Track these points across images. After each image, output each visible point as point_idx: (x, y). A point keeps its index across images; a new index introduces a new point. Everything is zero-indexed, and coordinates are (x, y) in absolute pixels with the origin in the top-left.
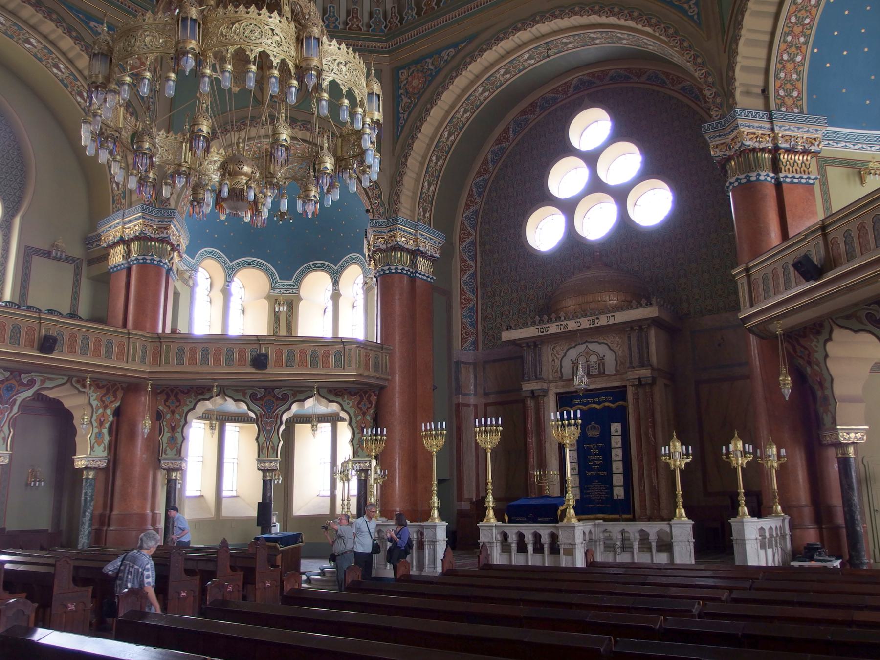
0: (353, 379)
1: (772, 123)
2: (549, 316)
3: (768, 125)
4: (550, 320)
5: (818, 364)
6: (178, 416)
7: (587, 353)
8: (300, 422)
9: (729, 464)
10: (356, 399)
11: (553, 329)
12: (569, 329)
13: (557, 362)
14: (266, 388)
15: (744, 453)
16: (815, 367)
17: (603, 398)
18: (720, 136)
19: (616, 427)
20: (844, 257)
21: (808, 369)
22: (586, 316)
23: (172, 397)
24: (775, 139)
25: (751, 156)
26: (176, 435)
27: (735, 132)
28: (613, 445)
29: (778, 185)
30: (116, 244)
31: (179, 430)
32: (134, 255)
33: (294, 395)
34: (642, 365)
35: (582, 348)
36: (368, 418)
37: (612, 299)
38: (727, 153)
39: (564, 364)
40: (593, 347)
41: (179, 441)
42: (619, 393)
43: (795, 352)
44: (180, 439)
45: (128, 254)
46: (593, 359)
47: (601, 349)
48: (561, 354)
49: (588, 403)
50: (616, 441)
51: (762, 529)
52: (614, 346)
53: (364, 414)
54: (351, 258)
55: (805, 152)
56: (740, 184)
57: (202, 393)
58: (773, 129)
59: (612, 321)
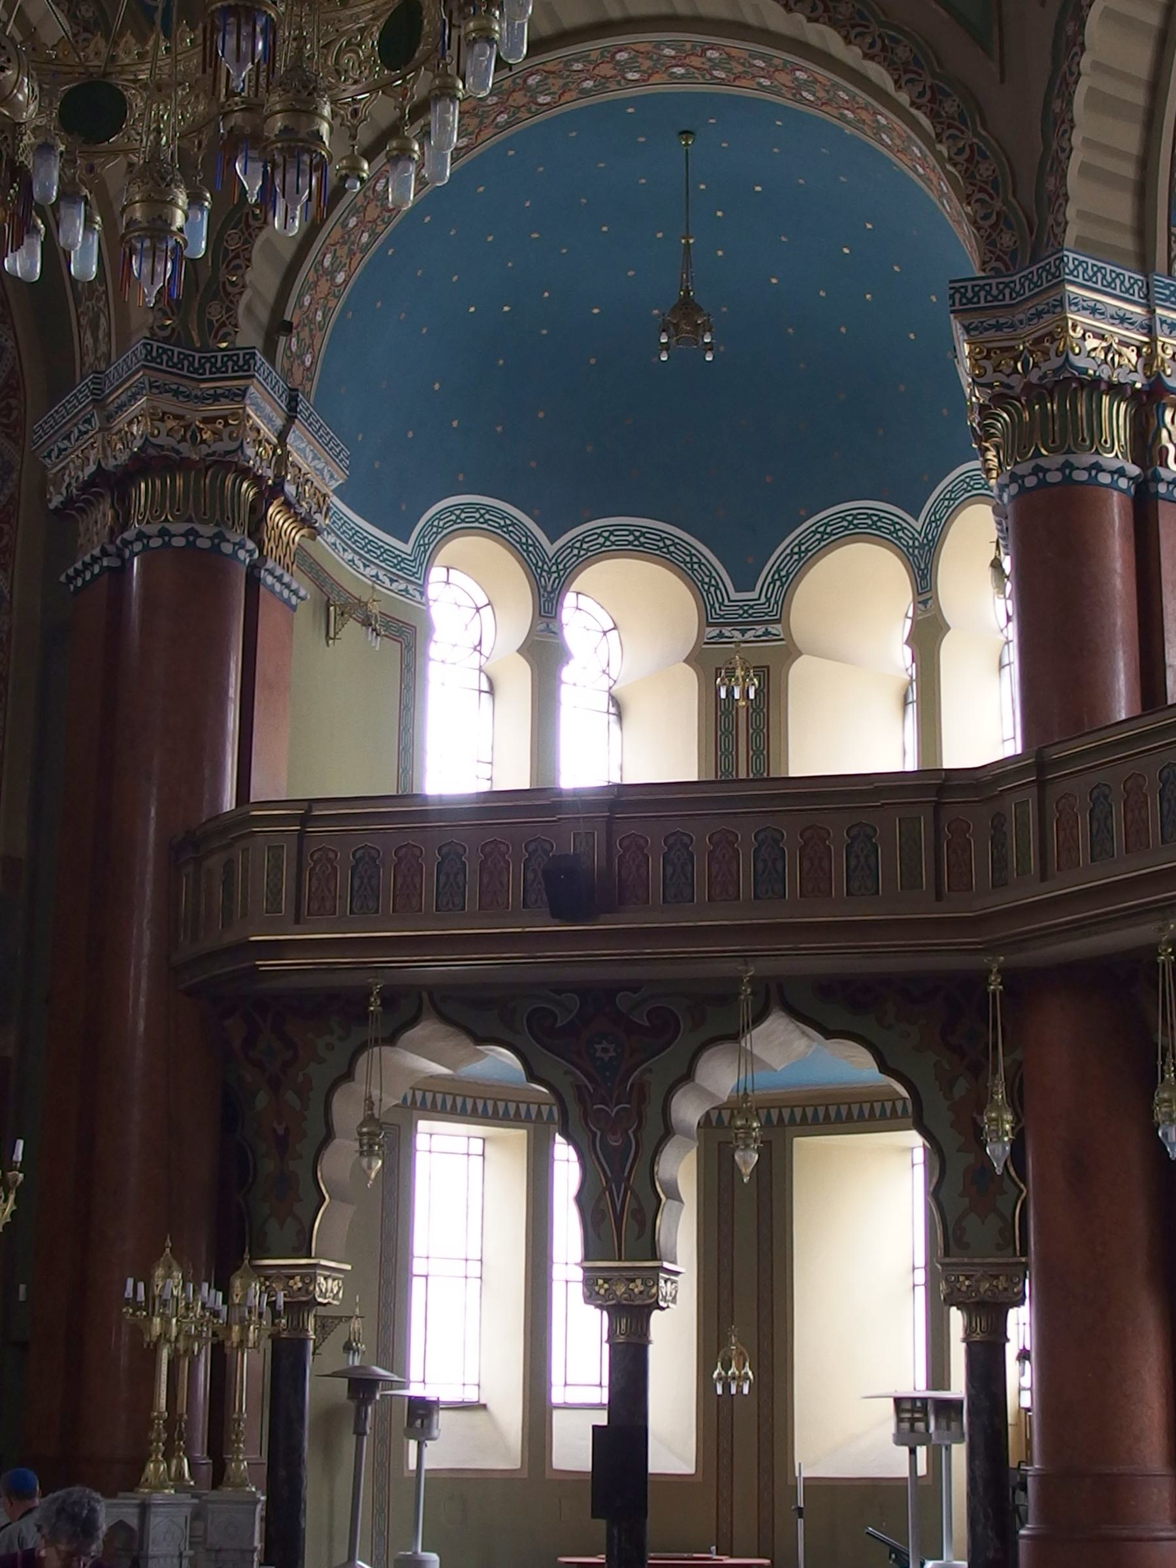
1: (290, 419)
3: (279, 422)
16: (290, 1097)
18: (176, 393)
21: (262, 1100)
24: (282, 462)
25: (229, 483)
27: (225, 406)
29: (253, 582)
38: (184, 448)
55: (305, 522)
56: (191, 545)
58: (282, 436)
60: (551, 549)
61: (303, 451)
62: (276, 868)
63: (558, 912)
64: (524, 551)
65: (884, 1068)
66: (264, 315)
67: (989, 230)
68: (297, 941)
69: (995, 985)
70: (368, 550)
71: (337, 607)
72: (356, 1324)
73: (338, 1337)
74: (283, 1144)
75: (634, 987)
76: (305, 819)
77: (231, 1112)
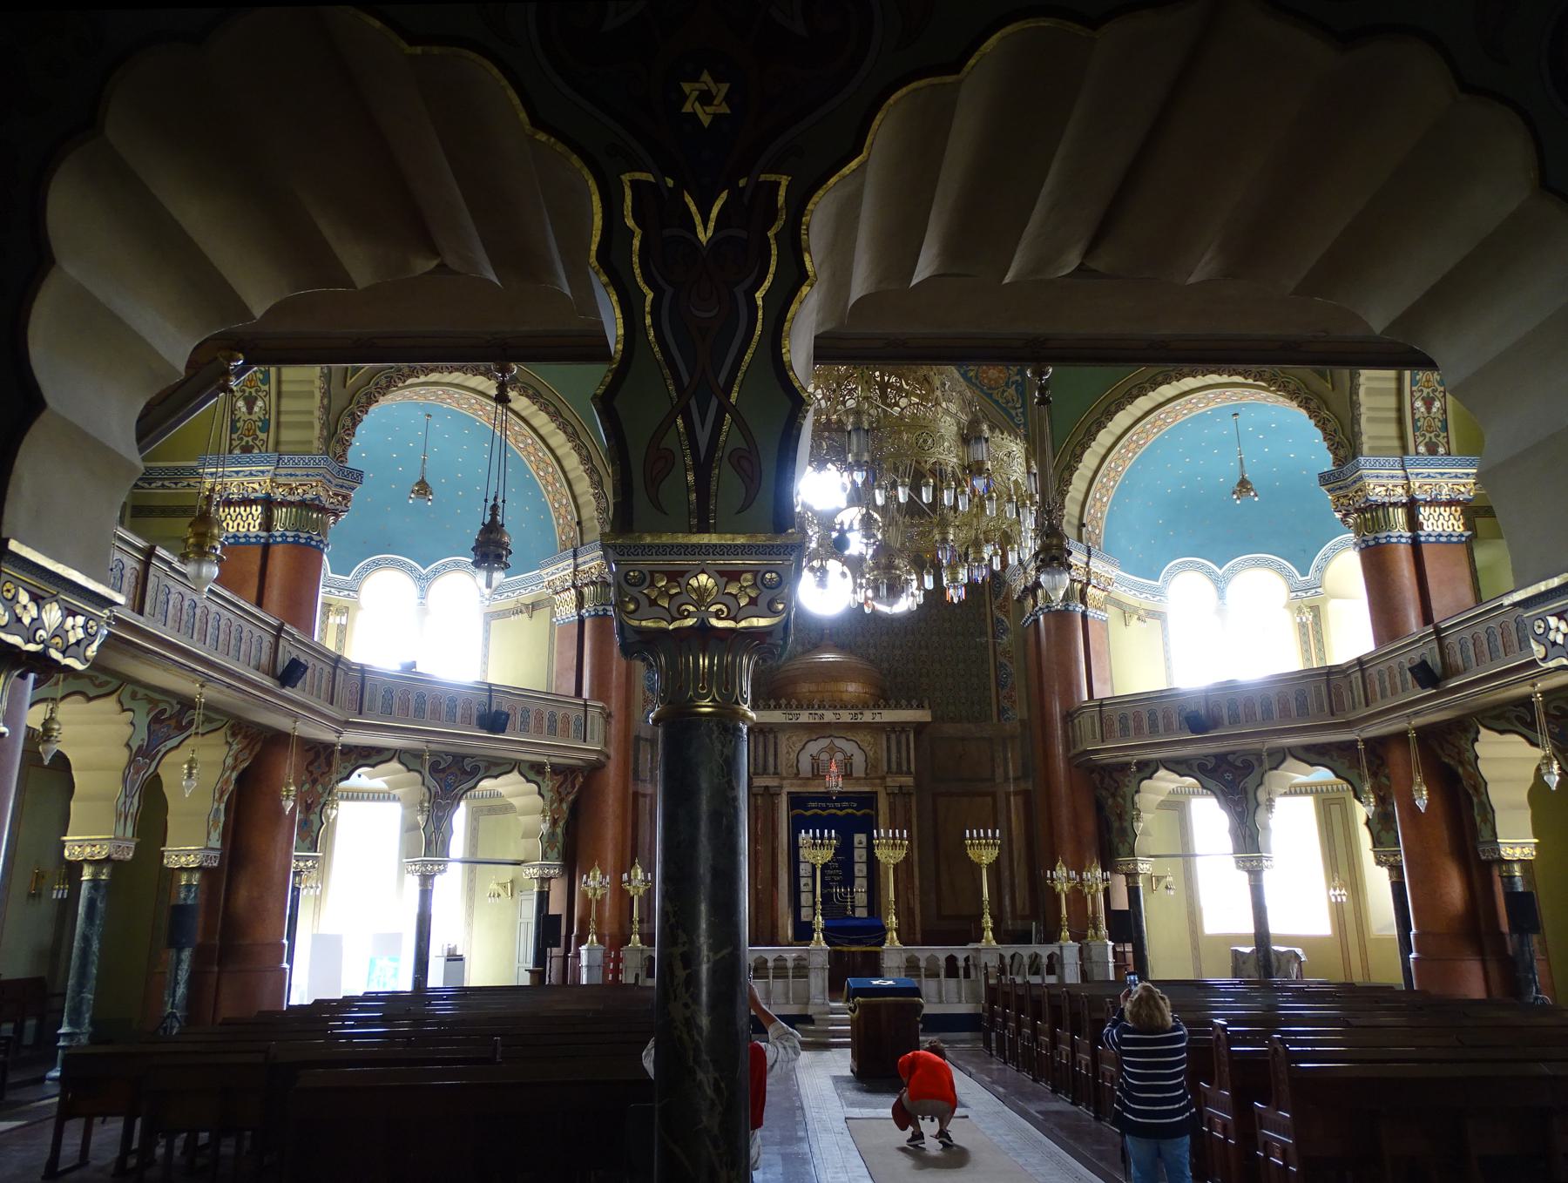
0: (594, 757)
2: (777, 699)
4: (800, 707)
5: (1124, 798)
6: (320, 788)
7: (832, 750)
8: (347, 799)
9: (1053, 889)
10: (560, 778)
11: (804, 717)
12: (826, 720)
13: (793, 756)
14: (455, 756)
15: (1069, 879)
17: (845, 804)
19: (860, 838)
20: (1226, 722)
21: (1110, 801)
22: (846, 708)
23: (322, 758)
24: (1088, 573)
26: (312, 817)
28: (856, 858)
29: (1084, 616)
30: (247, 502)
31: (317, 810)
32: (278, 529)
33: (487, 769)
34: (900, 772)
35: (824, 743)
36: (565, 806)
37: (852, 688)
39: (801, 758)
40: (839, 743)
41: (315, 829)
42: (868, 800)
43: (1102, 781)
44: (316, 824)
45: (267, 524)
46: (839, 756)
47: (849, 747)
48: (799, 746)
49: (827, 808)
50: (860, 854)
51: (1002, 957)
52: (864, 745)
53: (561, 801)
54: (457, 564)
57: (368, 756)
59: (878, 719)
60: (1220, 572)
61: (1097, 565)
62: (1093, 724)
63: (1193, 731)
64: (1210, 574)
65: (1338, 776)
66: (1076, 522)
67: (1334, 447)
68: (1107, 750)
69: (1361, 746)
70: (1141, 589)
71: (1126, 612)
72: (1170, 879)
73: (1162, 884)
74: (1120, 817)
75: (1233, 753)
76: (1101, 706)
77: (1099, 807)
